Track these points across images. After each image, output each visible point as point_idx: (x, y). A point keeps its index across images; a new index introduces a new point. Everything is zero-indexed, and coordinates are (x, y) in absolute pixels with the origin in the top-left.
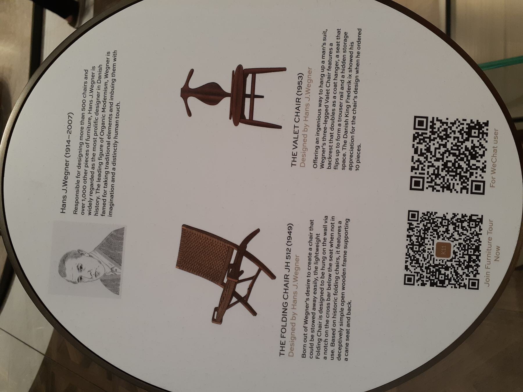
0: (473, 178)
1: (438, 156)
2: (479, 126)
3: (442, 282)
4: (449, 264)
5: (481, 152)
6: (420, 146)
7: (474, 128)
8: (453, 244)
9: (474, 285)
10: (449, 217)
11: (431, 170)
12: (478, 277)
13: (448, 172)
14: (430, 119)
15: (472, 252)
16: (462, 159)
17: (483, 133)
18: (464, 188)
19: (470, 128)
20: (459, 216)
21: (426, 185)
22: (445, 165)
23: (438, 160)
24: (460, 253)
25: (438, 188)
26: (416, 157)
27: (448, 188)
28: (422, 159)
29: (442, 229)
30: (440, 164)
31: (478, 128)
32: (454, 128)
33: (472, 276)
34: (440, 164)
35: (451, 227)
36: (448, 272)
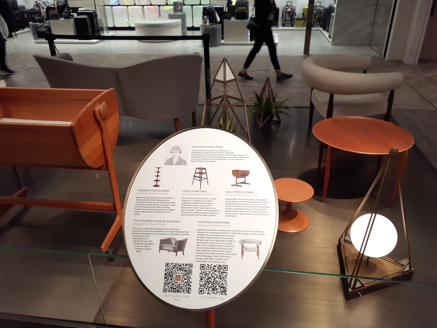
0: (205, 289)
1: (213, 275)
2: (225, 291)
3: (166, 278)
4: (173, 280)
5: (215, 292)
6: (216, 268)
7: (224, 289)
8: (180, 282)
9: (165, 290)
10: (190, 280)
11: (208, 272)
12: (168, 292)
13: (207, 279)
14: (227, 271)
15: (176, 289)
16: (212, 285)
17: (222, 293)
18: (201, 286)
19: (224, 288)
20: (190, 284)
21: (202, 270)
22: (210, 278)
23: (212, 275)
24: (177, 284)
25: (201, 275)
26: (212, 266)
27: (201, 279)
28: (212, 269)
29: (186, 277)
30: (210, 276)
31: (224, 291)
32: (224, 281)
33: (168, 289)
34: (210, 276)
35: (186, 281)
36: (170, 280)
